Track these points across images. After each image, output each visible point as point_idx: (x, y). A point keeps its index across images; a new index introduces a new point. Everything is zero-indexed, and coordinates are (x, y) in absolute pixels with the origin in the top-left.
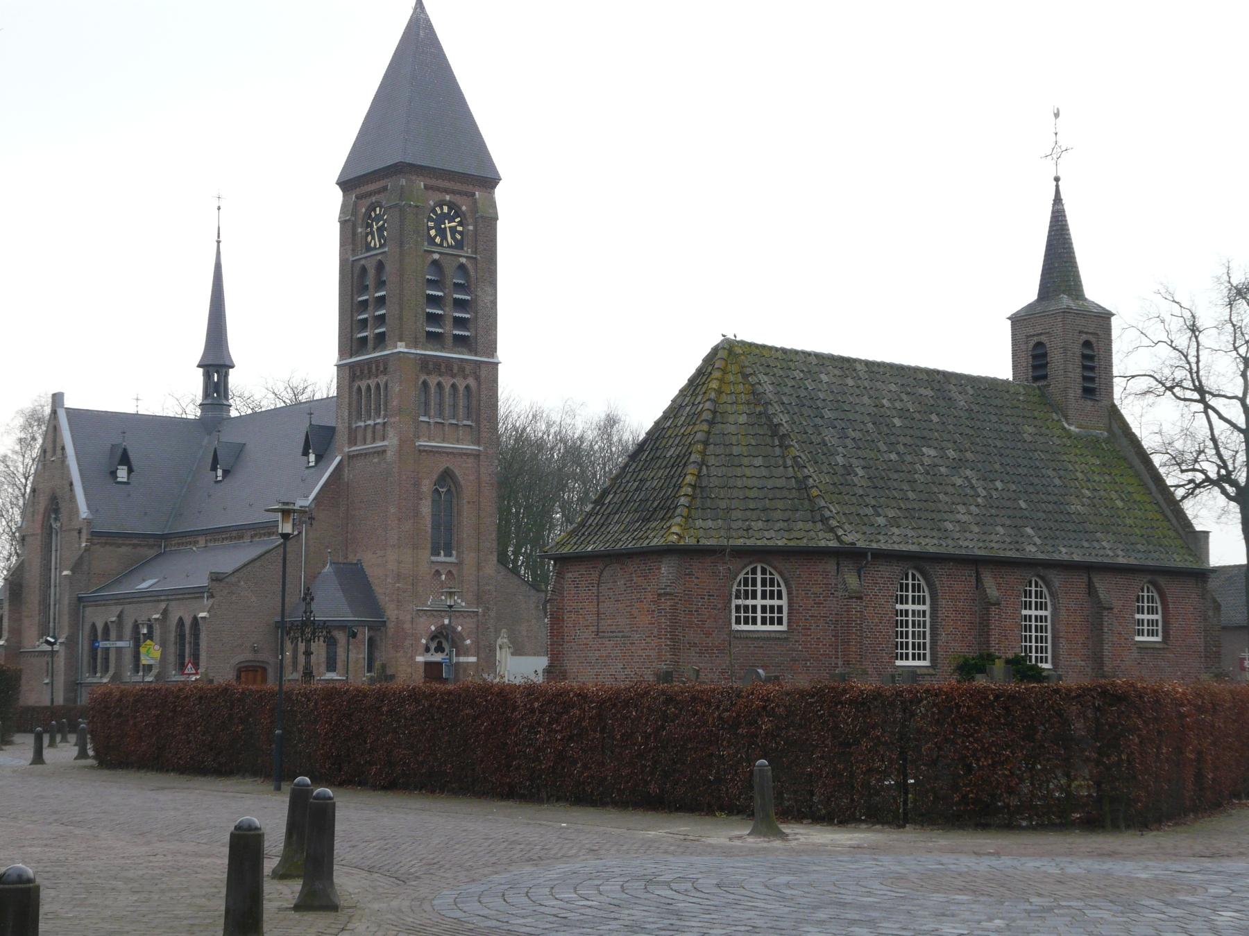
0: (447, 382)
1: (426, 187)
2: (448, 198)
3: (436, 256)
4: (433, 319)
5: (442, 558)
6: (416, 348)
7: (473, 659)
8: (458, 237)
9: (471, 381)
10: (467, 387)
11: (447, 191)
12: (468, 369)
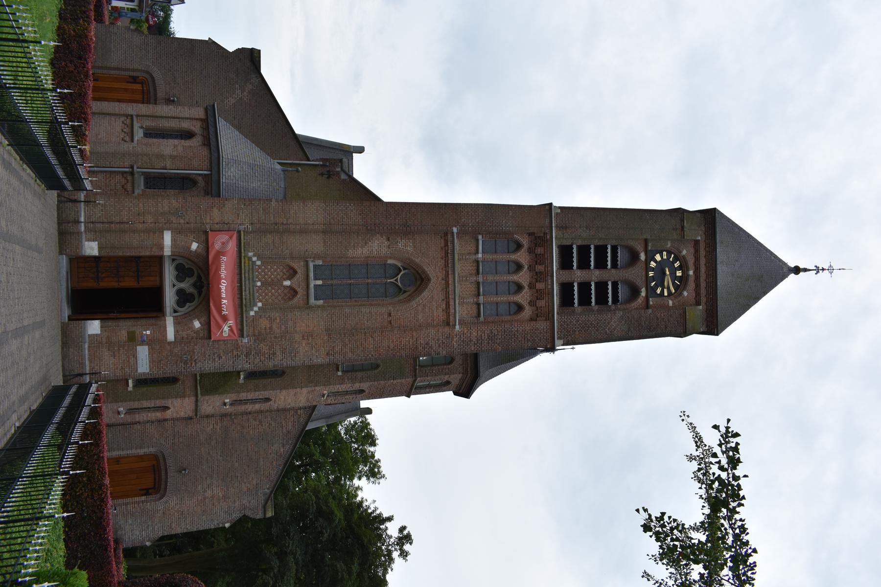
0: (523, 277)
1: (697, 242)
2: (691, 273)
3: (643, 257)
4: (584, 251)
5: (313, 283)
6: (557, 227)
7: (171, 334)
8: (659, 291)
9: (528, 312)
10: (520, 308)
11: (697, 270)
12: (541, 303)
